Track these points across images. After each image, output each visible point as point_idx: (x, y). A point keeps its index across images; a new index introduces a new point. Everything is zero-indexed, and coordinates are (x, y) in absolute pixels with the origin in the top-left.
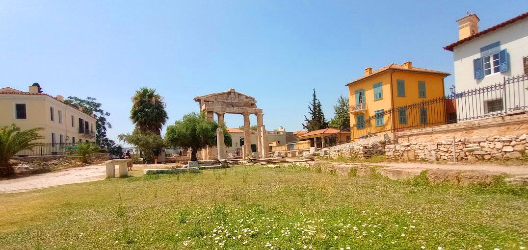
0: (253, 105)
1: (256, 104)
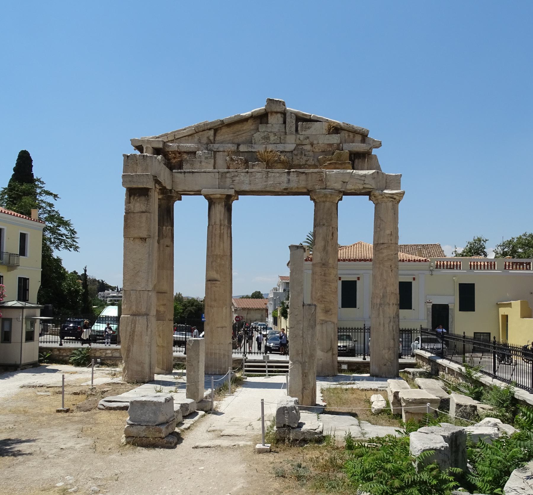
1: (374, 152)
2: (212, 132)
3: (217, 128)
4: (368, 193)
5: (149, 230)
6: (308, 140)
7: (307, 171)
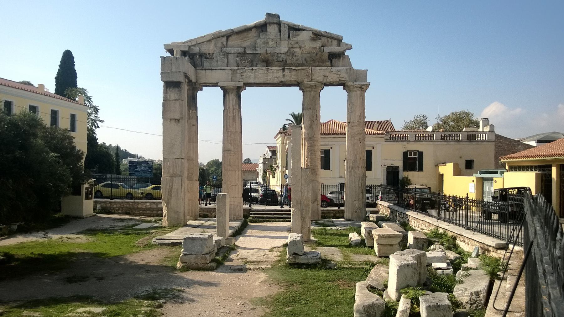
0: (339, 56)
1: (347, 53)
2: (225, 39)
3: (229, 35)
4: (343, 85)
5: (181, 114)
7: (297, 68)
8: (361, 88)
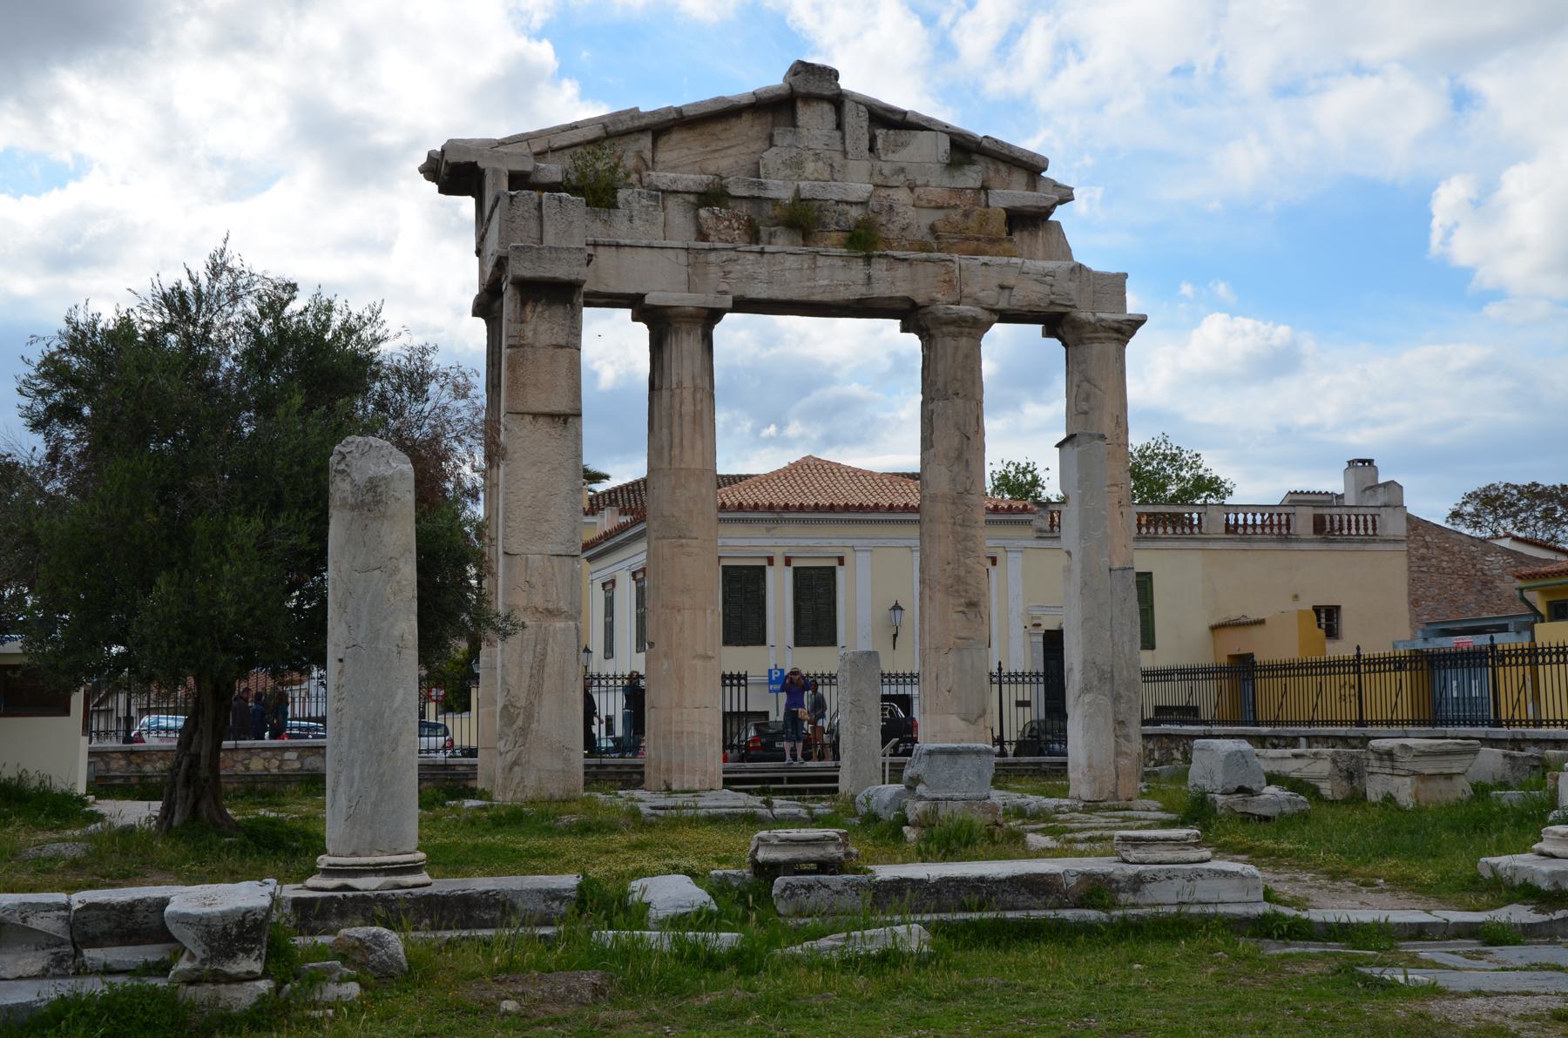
2: (646, 141)
6: (902, 177)
8: (1118, 331)
